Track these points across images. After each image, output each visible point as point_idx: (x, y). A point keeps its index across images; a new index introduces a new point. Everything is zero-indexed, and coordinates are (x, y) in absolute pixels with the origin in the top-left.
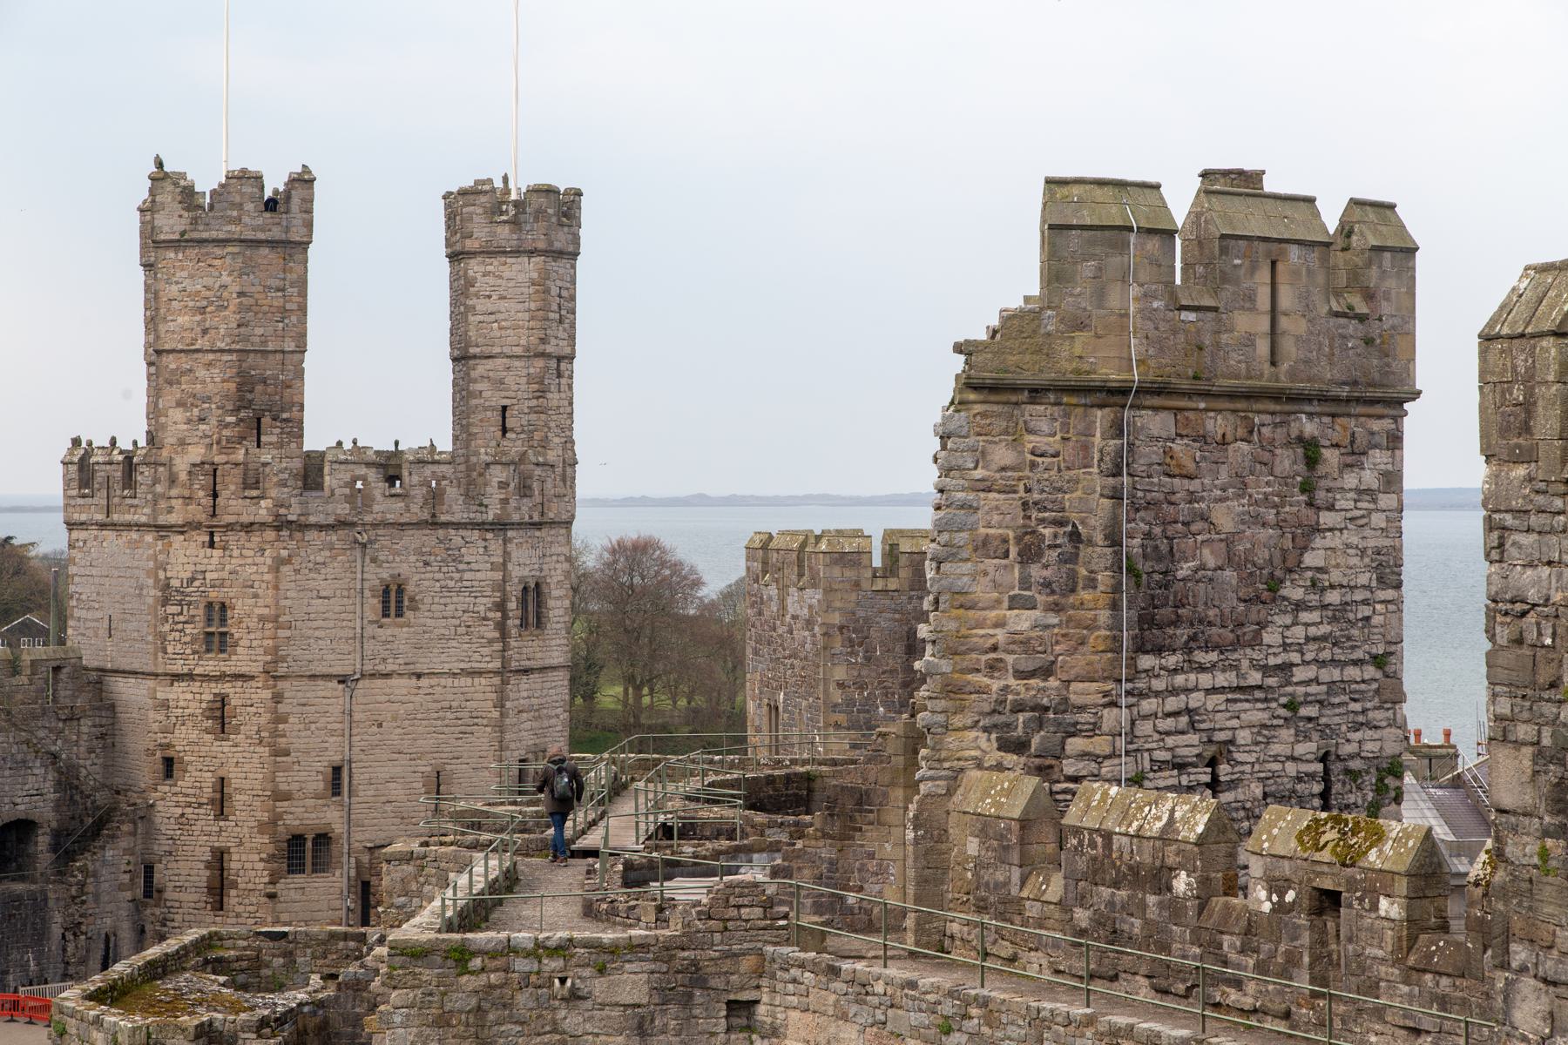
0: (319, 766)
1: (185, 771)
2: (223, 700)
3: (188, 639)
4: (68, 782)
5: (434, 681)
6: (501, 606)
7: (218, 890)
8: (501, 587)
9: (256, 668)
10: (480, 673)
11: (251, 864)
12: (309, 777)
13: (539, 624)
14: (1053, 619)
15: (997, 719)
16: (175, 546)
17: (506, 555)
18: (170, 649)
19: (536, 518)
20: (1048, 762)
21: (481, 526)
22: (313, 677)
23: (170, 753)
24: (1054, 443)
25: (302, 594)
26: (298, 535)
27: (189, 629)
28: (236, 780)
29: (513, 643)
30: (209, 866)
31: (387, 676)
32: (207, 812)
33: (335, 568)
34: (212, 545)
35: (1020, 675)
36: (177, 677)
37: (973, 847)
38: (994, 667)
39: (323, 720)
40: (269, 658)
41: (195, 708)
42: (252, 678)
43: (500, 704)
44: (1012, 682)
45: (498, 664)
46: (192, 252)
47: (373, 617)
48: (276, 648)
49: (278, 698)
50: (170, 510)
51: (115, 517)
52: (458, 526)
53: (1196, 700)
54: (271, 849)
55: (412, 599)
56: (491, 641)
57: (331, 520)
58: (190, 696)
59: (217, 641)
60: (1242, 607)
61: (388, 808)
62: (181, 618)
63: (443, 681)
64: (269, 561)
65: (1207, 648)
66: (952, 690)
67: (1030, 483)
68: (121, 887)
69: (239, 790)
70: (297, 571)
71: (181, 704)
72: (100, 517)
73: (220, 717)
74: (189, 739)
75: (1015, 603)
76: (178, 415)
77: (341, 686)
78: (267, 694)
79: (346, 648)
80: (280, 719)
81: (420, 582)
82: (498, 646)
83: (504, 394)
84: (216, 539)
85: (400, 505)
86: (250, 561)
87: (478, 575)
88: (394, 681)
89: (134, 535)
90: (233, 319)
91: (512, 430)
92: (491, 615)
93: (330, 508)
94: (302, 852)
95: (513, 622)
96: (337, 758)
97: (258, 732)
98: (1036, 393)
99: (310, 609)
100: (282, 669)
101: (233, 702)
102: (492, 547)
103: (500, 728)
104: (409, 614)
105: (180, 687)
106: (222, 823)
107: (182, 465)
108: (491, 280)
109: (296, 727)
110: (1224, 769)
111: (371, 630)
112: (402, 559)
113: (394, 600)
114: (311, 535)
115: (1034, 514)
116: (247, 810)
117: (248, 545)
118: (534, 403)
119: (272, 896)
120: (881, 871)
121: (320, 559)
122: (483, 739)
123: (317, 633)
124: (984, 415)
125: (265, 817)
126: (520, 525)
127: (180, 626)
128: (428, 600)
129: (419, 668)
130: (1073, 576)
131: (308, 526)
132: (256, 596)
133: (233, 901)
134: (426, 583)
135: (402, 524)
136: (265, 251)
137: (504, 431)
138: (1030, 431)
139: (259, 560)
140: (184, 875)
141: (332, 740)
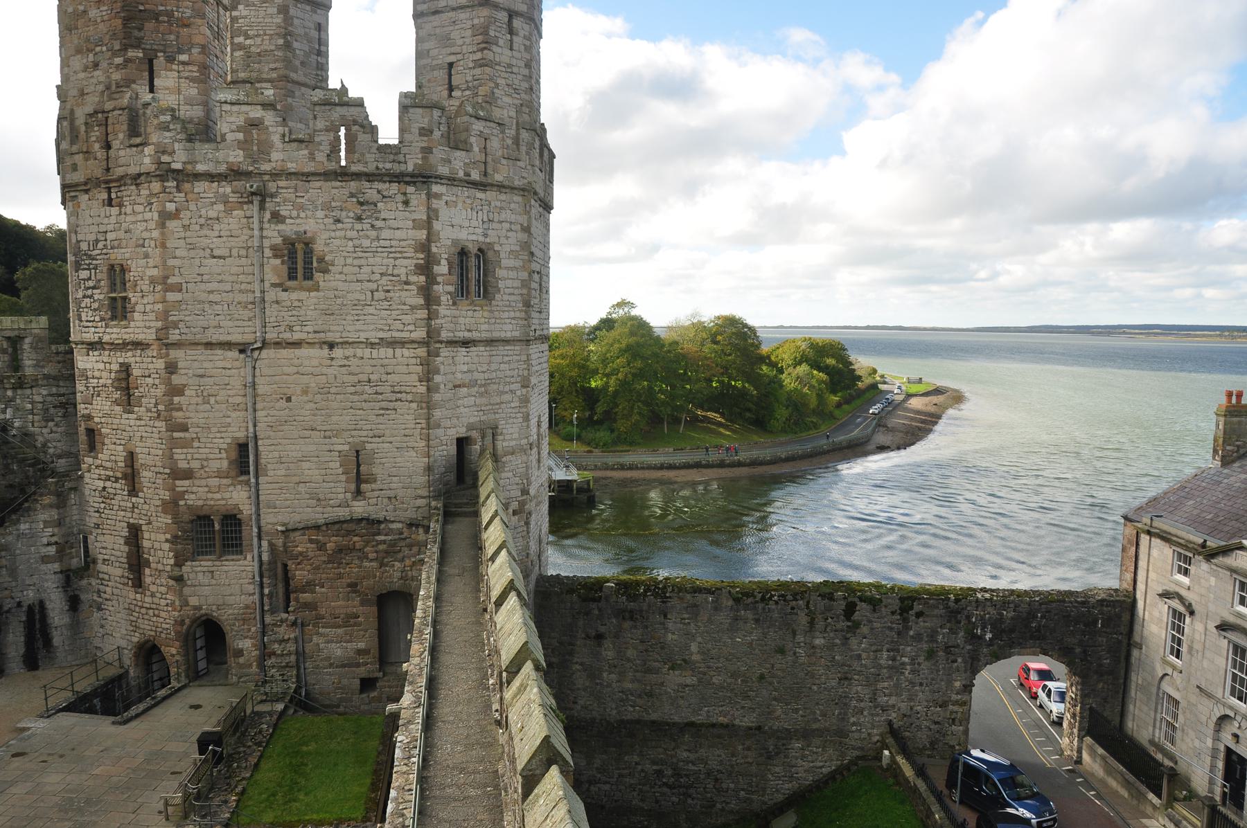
1: (103, 444)
2: (126, 369)
3: (96, 305)
5: (349, 352)
6: (426, 268)
8: (425, 247)
9: (149, 336)
10: (402, 343)
12: (212, 453)
16: (83, 206)
17: (432, 215)
18: (83, 315)
19: (475, 176)
21: (398, 178)
22: (209, 345)
23: (91, 425)
25: (192, 253)
26: (187, 186)
28: (141, 459)
29: (443, 311)
31: (297, 344)
34: (110, 203)
39: (222, 393)
40: (159, 324)
41: (106, 379)
43: (427, 377)
45: (424, 334)
47: (275, 280)
48: (166, 313)
49: (172, 368)
52: (370, 177)
56: (413, 308)
57: (223, 168)
58: (101, 366)
61: (302, 488)
63: (359, 352)
68: (45, 559)
71: (97, 374)
77: (242, 356)
78: (160, 364)
79: (246, 314)
81: (330, 240)
82: (423, 314)
83: (449, 50)
84: (113, 196)
86: (140, 217)
87: (398, 234)
88: (304, 352)
91: (458, 87)
92: (413, 278)
93: (220, 155)
94: (213, 533)
95: (443, 289)
96: (241, 435)
97: (156, 404)
99: (203, 270)
100: (174, 336)
101: (136, 372)
102: (413, 202)
103: (428, 405)
104: (318, 276)
106: (134, 499)
109: (194, 400)
112: (310, 215)
113: (300, 261)
114: (200, 186)
116: (154, 489)
117: (139, 200)
118: (479, 55)
121: (212, 214)
122: (408, 415)
123: (212, 297)
125: (166, 495)
126: (452, 181)
127: (89, 292)
128: (339, 261)
129: (330, 337)
131: (197, 176)
132: (146, 256)
133: (148, 580)
134: (337, 242)
135: (308, 175)
139: (148, 216)
141: (234, 415)
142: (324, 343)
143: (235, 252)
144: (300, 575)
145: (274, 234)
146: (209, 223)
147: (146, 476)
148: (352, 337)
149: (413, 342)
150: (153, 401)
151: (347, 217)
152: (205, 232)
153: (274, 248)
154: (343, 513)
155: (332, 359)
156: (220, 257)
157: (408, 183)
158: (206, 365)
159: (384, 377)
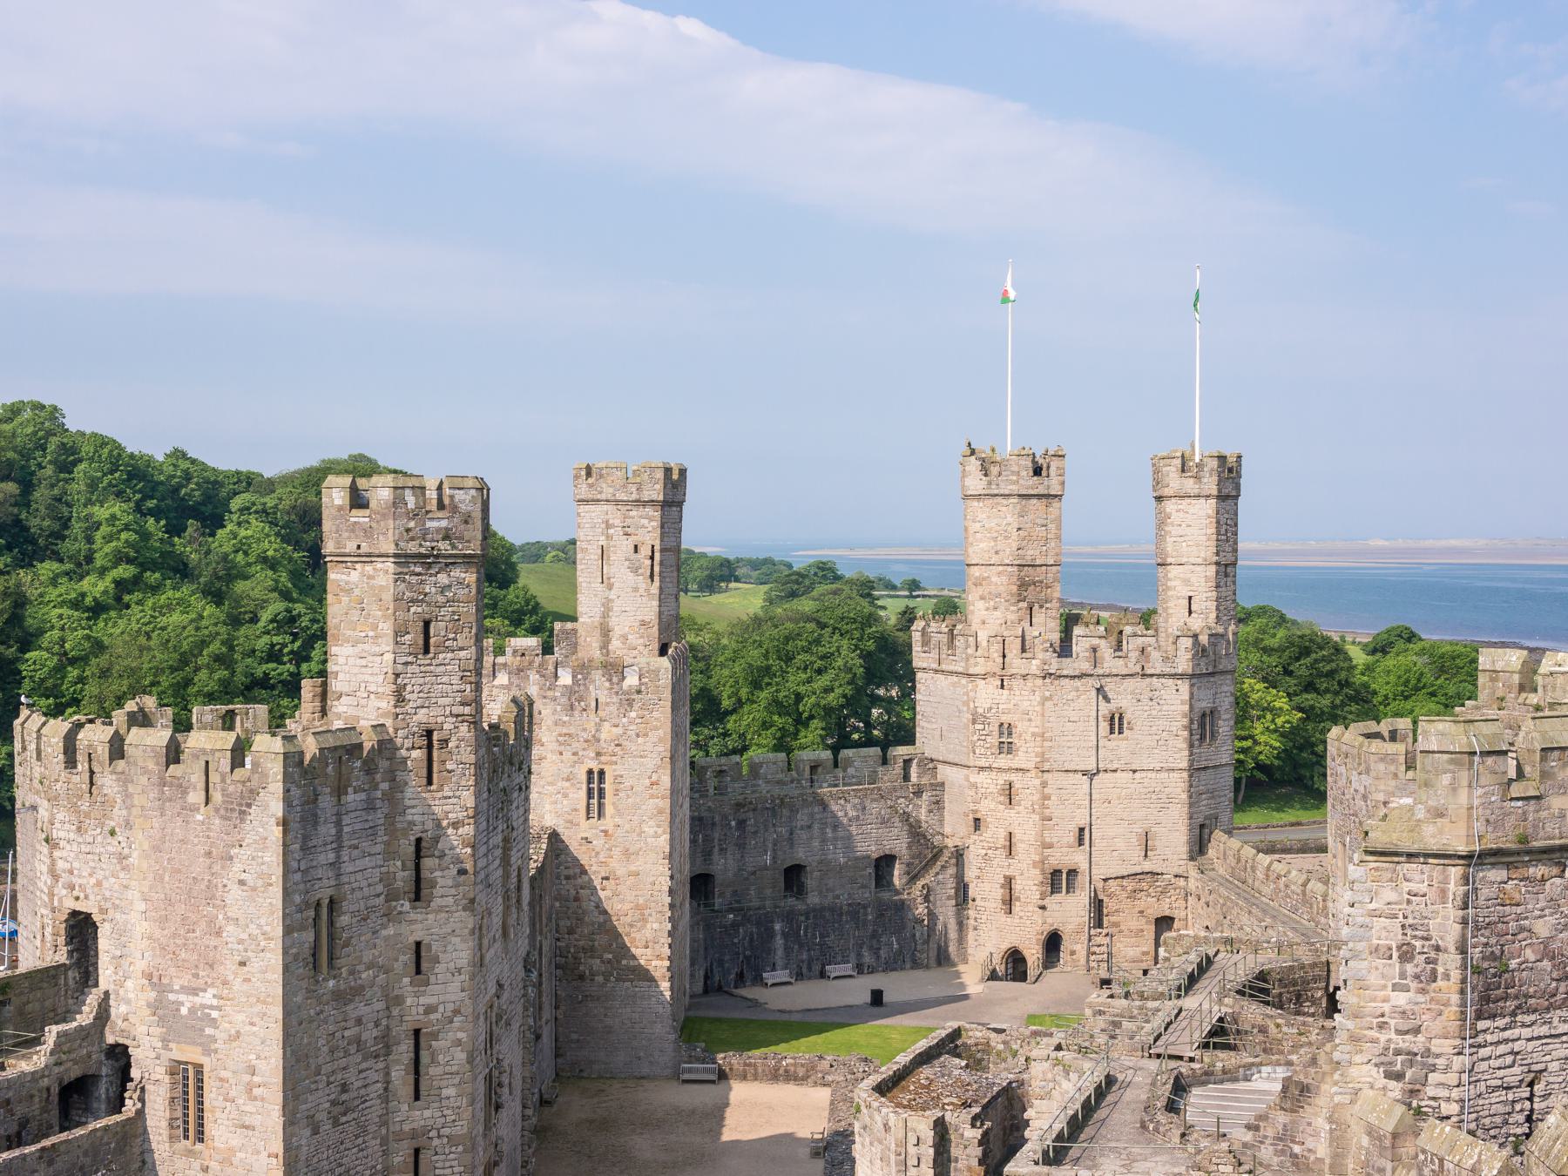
0: (1071, 827)
4: (916, 833)
5: (1144, 774)
7: (1009, 902)
9: (1031, 765)
11: (1029, 885)
13: (1213, 737)
14: (1421, 998)
15: (1383, 1059)
20: (1418, 1087)
24: (1423, 888)
30: (1003, 886)
32: (1002, 853)
35: (1399, 1032)
36: (982, 769)
37: (1365, 1141)
38: (1382, 1026)
41: (993, 789)
44: (1393, 1036)
46: (990, 502)
49: (1044, 784)
50: (976, 665)
51: (944, 667)
52: (1159, 676)
53: (1517, 1046)
54: (1040, 878)
57: (1077, 673)
59: (1006, 748)
60: (1554, 984)
65: (1529, 1011)
66: (1355, 1039)
67: (1408, 913)
68: (949, 898)
69: (1022, 841)
72: (935, 666)
73: (1009, 793)
74: (991, 808)
75: (1395, 988)
76: (980, 605)
78: (1037, 782)
80: (1046, 797)
85: (1121, 661)
89: (955, 679)
90: (1015, 546)
94: (1058, 880)
96: (1084, 822)
98: (1411, 856)
105: (984, 775)
107: (983, 637)
108: (1181, 514)
110: (1539, 1088)
113: (1116, 723)
115: (1409, 932)
119: (1043, 908)
120: (1316, 1135)
124: (1377, 869)
125: (1037, 858)
130: (1434, 972)
136: (1034, 501)
137: (1190, 612)
138: (1407, 880)
140: (985, 892)
144: (1109, 905)
147: (1020, 847)
151: (1145, 701)
154: (1138, 869)
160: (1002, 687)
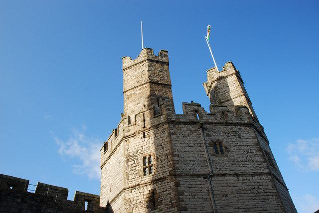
3: (137, 172)
5: (245, 178)
18: (130, 178)
22: (192, 175)
25: (181, 145)
26: (177, 126)
27: (137, 168)
31: (224, 175)
33: (194, 136)
42: (165, 178)
47: (212, 153)
55: (226, 148)
56: (261, 163)
62: (134, 165)
63: (248, 178)
64: (167, 135)
70: (178, 137)
71: (136, 198)
78: (173, 184)
81: (228, 141)
88: (228, 178)
97: (171, 201)
100: (178, 172)
101: (158, 192)
109: (189, 197)
111: (212, 158)
114: (181, 126)
123: (190, 159)
127: (134, 168)
129: (236, 172)
132: (163, 148)
142: (235, 174)
143: (196, 145)
145: (209, 140)
146: (185, 136)
148: (244, 172)
149: (266, 174)
150: (169, 200)
152: (184, 139)
153: (209, 144)
155: (239, 180)
156: (191, 146)
157: (246, 126)
158: (192, 183)
159: (260, 187)
160: (144, 137)
